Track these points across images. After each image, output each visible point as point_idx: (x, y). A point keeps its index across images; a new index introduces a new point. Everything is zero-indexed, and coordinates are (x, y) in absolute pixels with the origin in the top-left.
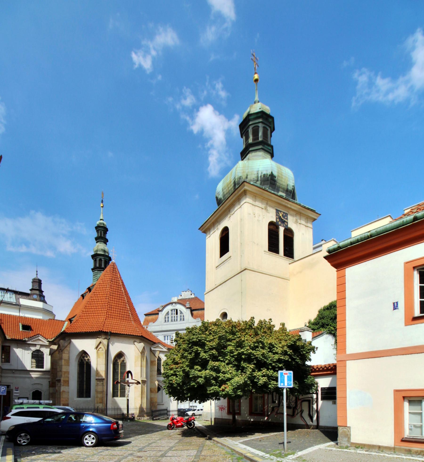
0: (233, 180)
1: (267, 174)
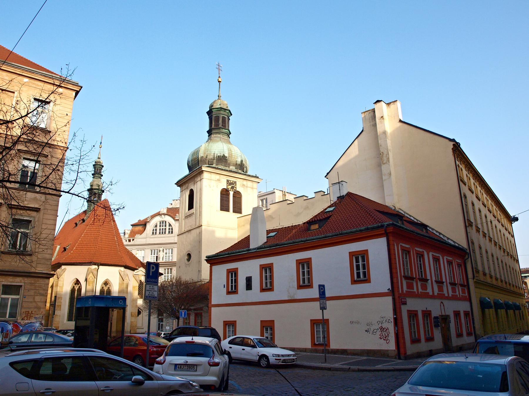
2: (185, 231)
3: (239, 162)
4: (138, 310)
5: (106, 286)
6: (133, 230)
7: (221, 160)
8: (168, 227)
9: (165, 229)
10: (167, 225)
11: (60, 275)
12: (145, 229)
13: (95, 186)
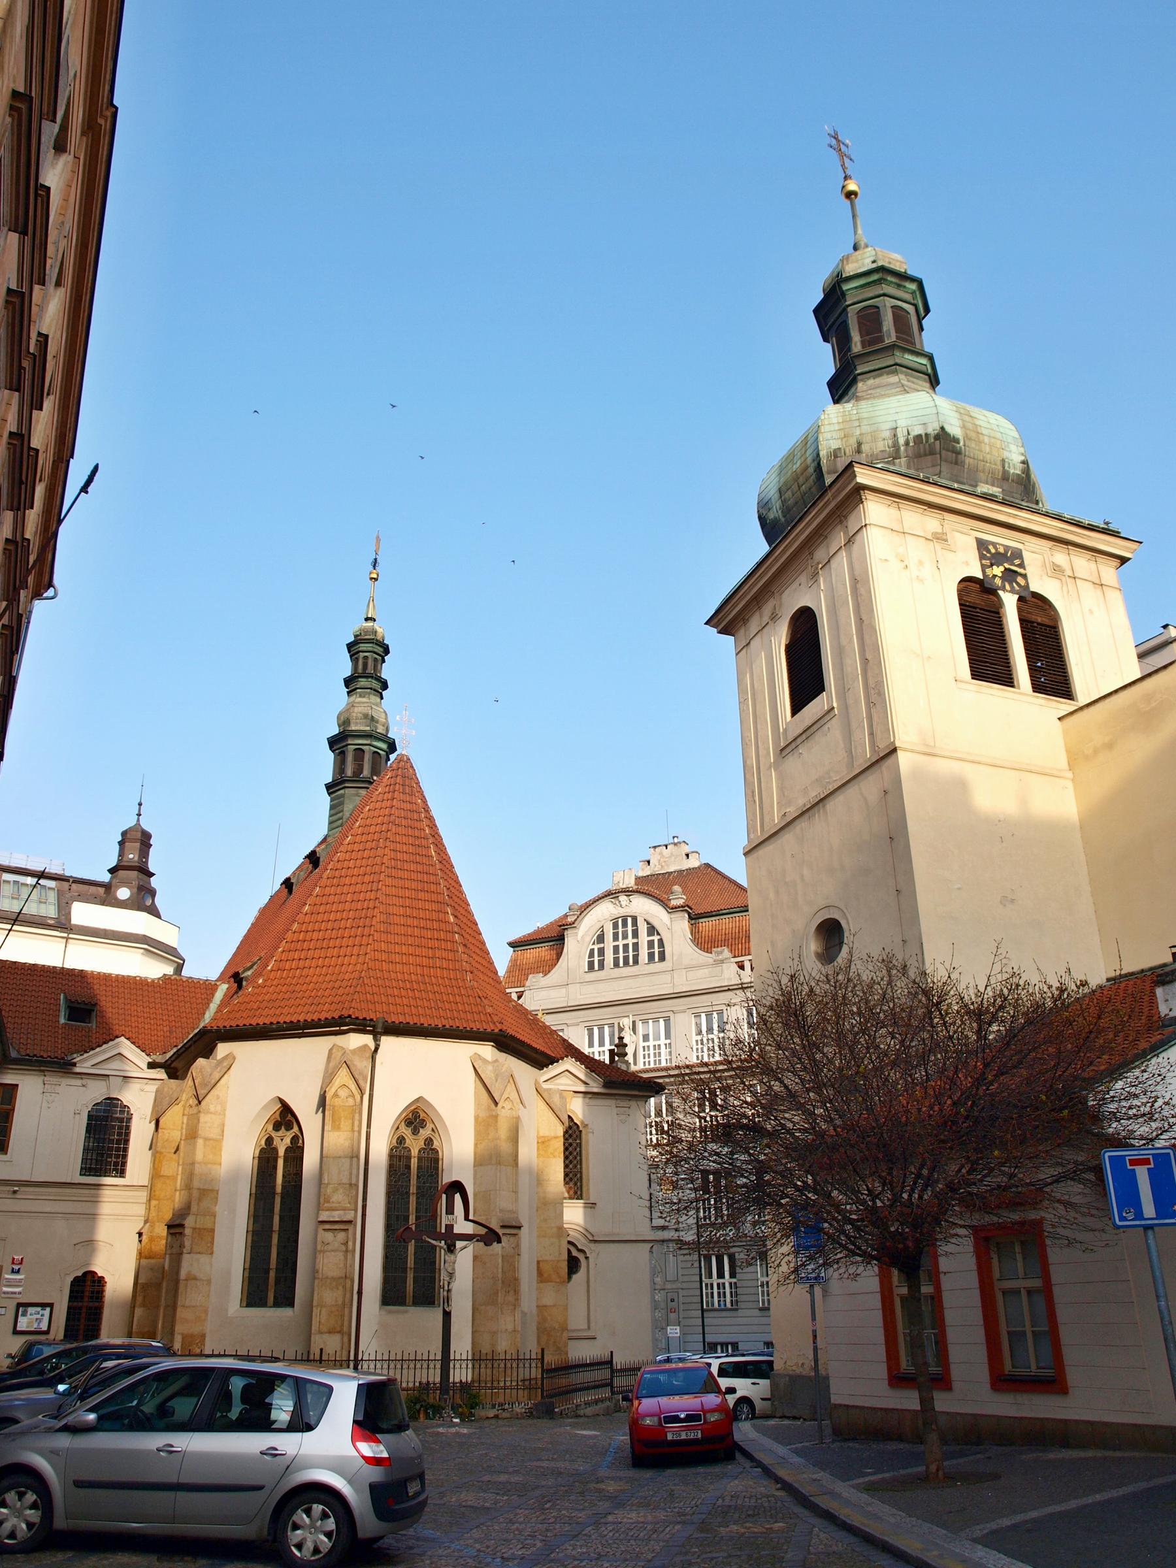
0: (814, 461)
2: (789, 819)
3: (1016, 469)
4: (569, 1251)
5: (415, 1132)
6: (516, 960)
7: (932, 453)
8: (644, 938)
9: (636, 946)
10: (643, 929)
11: (206, 1085)
12: (562, 953)
13: (356, 724)
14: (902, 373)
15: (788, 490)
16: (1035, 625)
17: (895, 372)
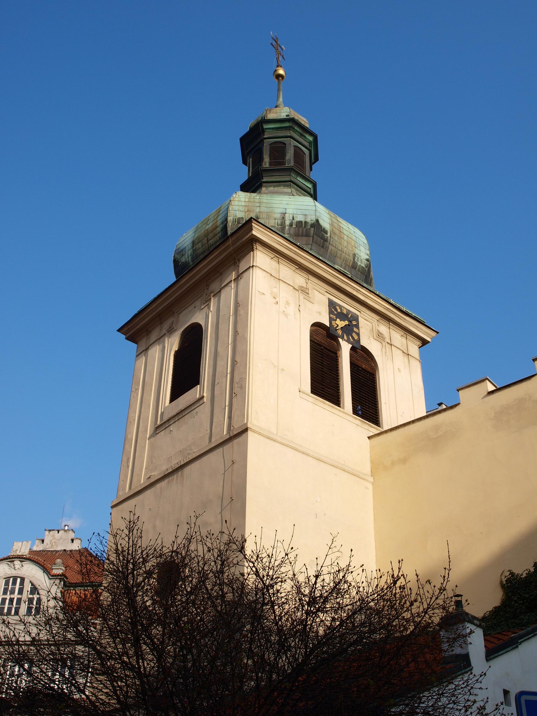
0: (222, 223)
1: (306, 222)
7: (307, 235)
14: (294, 188)
15: (199, 242)
16: (360, 369)
17: (290, 186)
